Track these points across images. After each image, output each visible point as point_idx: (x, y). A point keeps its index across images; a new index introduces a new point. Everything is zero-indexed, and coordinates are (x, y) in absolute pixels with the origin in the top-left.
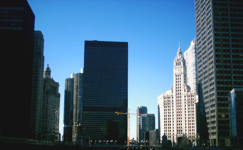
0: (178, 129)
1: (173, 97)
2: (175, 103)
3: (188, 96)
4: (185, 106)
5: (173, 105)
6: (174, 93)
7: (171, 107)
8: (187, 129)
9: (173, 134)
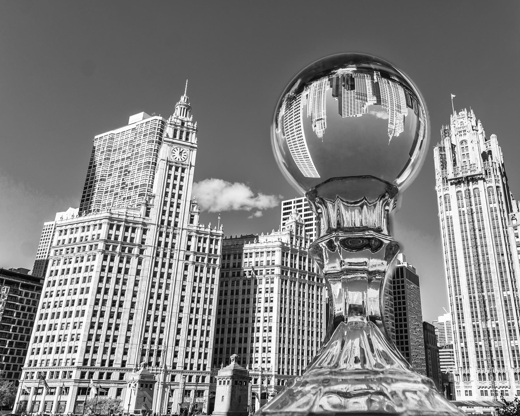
0: (147, 347)
1: (145, 232)
2: (149, 252)
3: (200, 238)
4: (186, 268)
5: (141, 256)
6: (154, 217)
7: (134, 261)
8: (181, 349)
9: (124, 363)
